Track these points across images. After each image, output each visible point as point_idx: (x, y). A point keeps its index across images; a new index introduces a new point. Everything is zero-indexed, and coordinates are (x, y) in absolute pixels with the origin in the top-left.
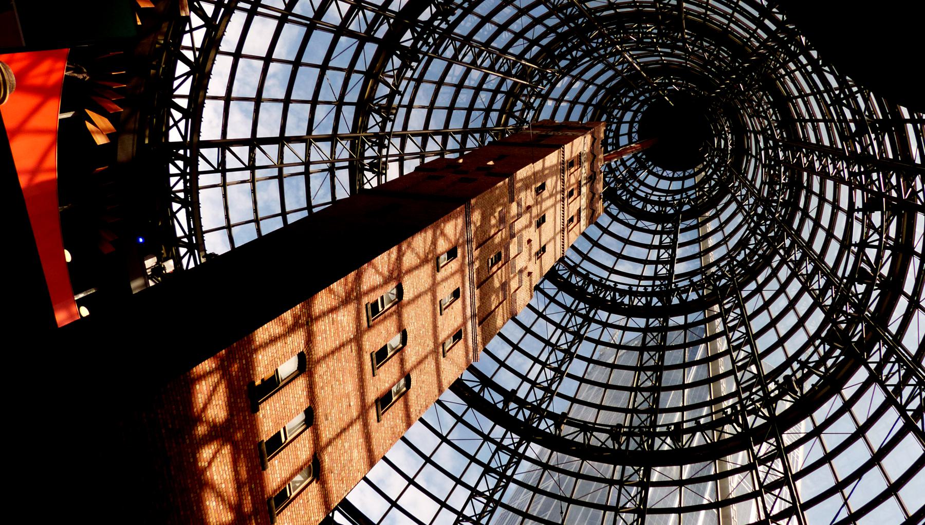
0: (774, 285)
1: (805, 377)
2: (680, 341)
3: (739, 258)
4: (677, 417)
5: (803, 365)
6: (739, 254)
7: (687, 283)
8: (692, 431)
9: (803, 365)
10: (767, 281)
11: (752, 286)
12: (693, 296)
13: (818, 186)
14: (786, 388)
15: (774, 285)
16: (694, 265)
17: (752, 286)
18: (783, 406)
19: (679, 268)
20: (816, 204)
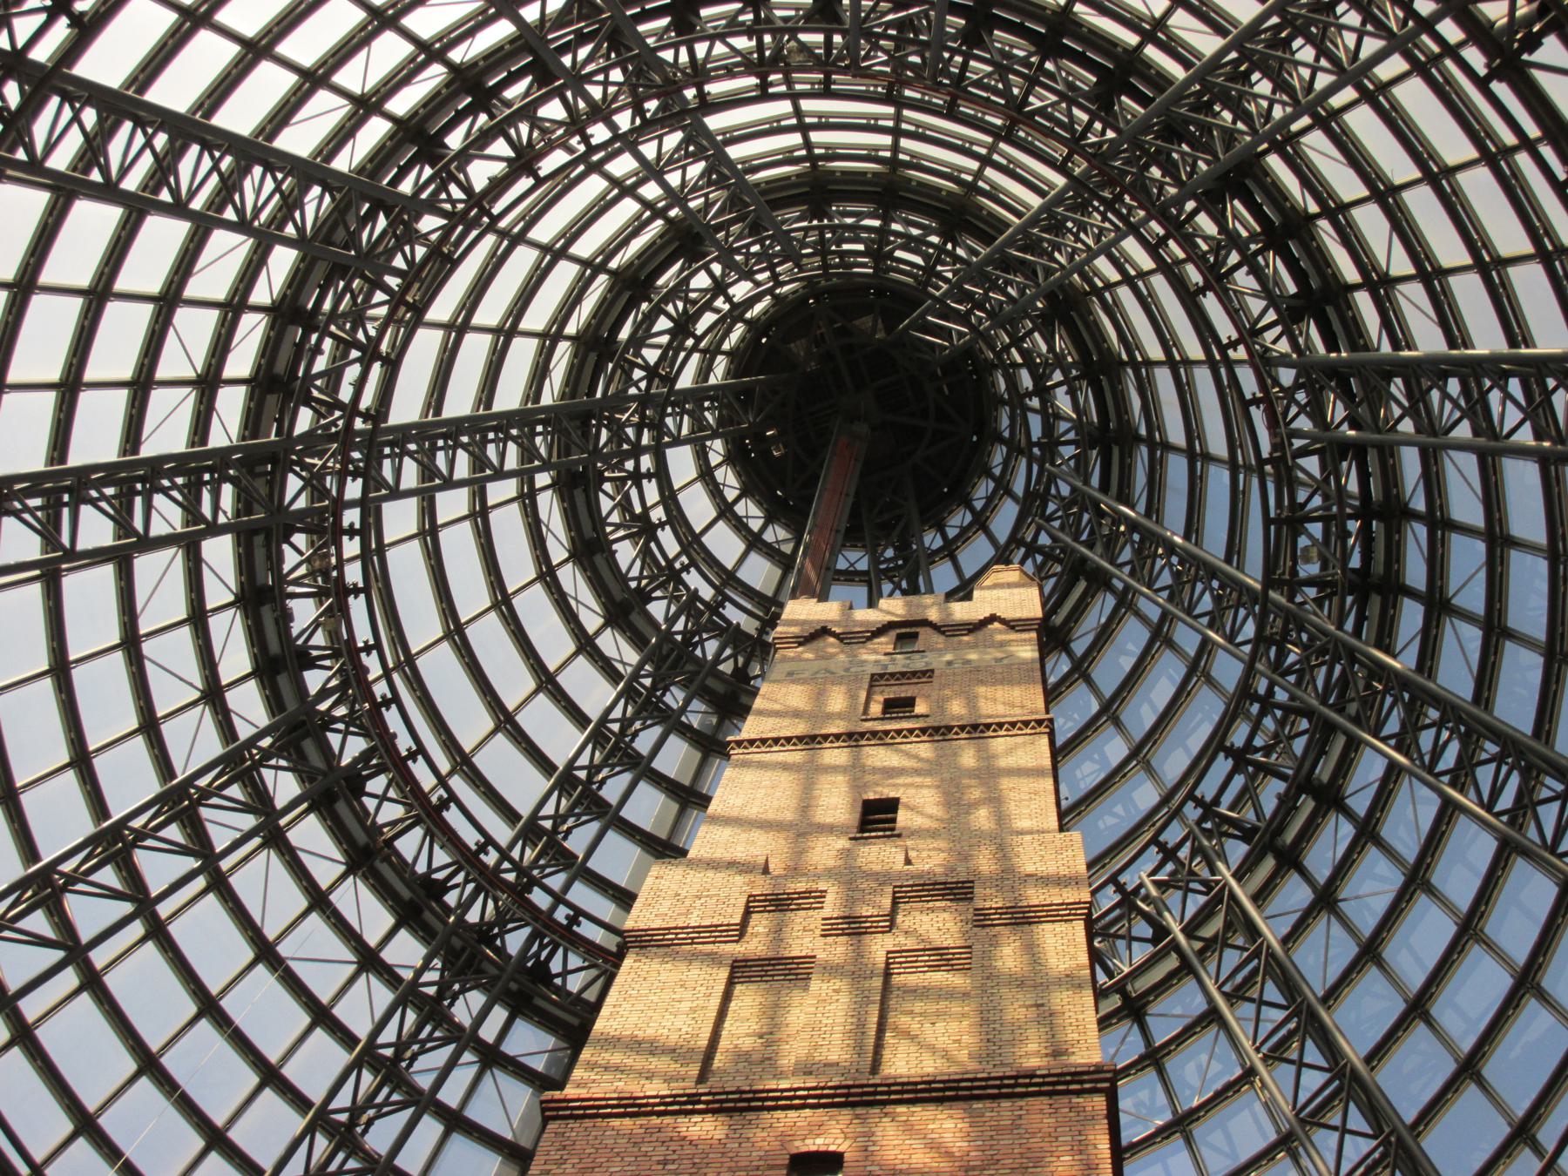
0: (1467, 556)
2: (1345, 950)
7: (1222, 765)
10: (1437, 563)
12: (1271, 792)
13: (1350, 174)
15: (1467, 556)
20: (1385, 225)
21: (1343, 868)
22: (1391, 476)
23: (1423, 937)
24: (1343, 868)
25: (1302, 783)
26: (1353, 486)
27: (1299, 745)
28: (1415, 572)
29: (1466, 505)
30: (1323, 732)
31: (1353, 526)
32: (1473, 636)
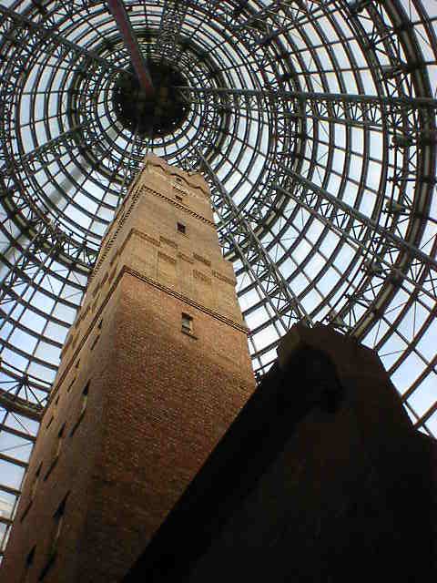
0: (323, 150)
1: (402, 188)
3: (280, 150)
4: (326, 310)
5: (395, 180)
6: (277, 146)
7: (252, 202)
8: (348, 309)
9: (395, 180)
11: (306, 165)
12: (264, 210)
14: (395, 211)
15: (323, 150)
16: (246, 188)
17: (306, 165)
18: (403, 228)
19: (238, 199)
21: (283, 231)
22: (304, 127)
23: (303, 250)
24: (283, 231)
25: (273, 208)
26: (293, 129)
27: (273, 198)
28: (308, 154)
29: (324, 136)
30: (280, 194)
31: (293, 139)
32: (323, 172)
